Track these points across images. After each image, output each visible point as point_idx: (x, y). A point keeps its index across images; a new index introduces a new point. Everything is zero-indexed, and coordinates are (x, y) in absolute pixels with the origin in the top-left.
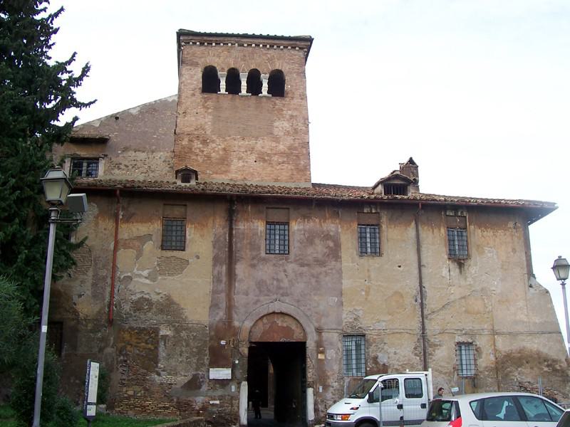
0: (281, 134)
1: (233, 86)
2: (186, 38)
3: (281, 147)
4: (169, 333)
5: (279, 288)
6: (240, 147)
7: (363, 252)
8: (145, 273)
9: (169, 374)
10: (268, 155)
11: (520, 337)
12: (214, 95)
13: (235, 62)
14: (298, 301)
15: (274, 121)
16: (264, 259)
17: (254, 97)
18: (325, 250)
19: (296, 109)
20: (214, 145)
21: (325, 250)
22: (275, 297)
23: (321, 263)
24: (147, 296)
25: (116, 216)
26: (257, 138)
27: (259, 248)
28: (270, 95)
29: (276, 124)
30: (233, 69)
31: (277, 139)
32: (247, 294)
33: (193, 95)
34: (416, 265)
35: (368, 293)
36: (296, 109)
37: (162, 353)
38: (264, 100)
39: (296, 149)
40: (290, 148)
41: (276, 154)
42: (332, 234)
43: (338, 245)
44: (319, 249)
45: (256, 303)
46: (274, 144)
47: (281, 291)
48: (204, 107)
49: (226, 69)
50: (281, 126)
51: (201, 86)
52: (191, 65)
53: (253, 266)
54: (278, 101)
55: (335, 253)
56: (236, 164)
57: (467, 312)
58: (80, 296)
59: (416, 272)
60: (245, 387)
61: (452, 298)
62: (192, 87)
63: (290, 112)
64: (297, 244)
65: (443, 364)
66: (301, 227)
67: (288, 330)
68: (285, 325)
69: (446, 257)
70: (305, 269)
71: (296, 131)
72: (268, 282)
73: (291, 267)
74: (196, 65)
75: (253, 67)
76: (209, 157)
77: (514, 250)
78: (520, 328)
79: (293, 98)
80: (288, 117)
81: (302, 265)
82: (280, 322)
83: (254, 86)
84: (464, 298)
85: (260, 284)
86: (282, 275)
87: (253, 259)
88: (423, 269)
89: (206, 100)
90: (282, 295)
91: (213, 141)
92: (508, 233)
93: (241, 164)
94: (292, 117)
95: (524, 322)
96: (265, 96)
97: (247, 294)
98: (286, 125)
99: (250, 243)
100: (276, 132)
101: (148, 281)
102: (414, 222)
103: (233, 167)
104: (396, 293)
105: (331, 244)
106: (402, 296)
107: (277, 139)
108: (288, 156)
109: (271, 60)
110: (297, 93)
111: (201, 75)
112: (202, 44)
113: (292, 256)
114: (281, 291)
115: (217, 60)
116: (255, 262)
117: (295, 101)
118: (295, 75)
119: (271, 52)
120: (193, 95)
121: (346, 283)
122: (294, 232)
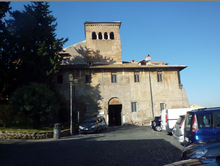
0: (114, 50)
1: (100, 37)
2: (87, 24)
3: (114, 53)
4: (89, 104)
5: (116, 91)
6: (103, 54)
7: (135, 81)
8: (82, 89)
9: (89, 114)
10: (111, 56)
11: (177, 101)
12: (95, 40)
13: (100, 31)
14: (120, 94)
16: (111, 84)
17: (106, 40)
18: (126, 81)
19: (117, 43)
21: (126, 81)
22: (114, 93)
23: (126, 85)
24: (83, 95)
26: (107, 51)
27: (110, 82)
28: (110, 39)
29: (112, 47)
30: (100, 32)
31: (113, 51)
32: (107, 93)
34: (149, 84)
35: (137, 92)
36: (117, 43)
37: (87, 108)
38: (109, 41)
39: (118, 54)
40: (116, 54)
41: (112, 55)
42: (128, 77)
43: (129, 80)
44: (125, 81)
45: (110, 95)
46: (112, 53)
47: (116, 92)
48: (93, 43)
49: (98, 32)
50: (114, 47)
51: (92, 37)
52: (89, 32)
53: (108, 86)
54: (112, 41)
55: (128, 82)
57: (163, 95)
58: (66, 96)
59: (149, 86)
60: (108, 116)
61: (159, 92)
62: (90, 38)
63: (116, 44)
64: (119, 80)
65: (157, 109)
66: (120, 76)
67: (117, 102)
68: (117, 100)
69: (157, 82)
70: (121, 86)
71: (118, 49)
72: (112, 90)
73: (118, 86)
74: (90, 32)
75: (105, 31)
78: (176, 99)
79: (116, 40)
80: (115, 45)
81: (120, 85)
82: (115, 99)
83: (106, 37)
84: (162, 92)
85: (110, 90)
86: (116, 88)
87: (108, 84)
88: (151, 85)
89: (93, 41)
90: (116, 93)
92: (173, 75)
94: (116, 45)
95: (178, 98)
96: (109, 40)
97: (107, 93)
98: (115, 47)
99: (107, 80)
100: (113, 49)
101: (83, 91)
102: (148, 73)
104: (144, 91)
105: (127, 80)
106: (146, 92)
107: (113, 51)
108: (116, 56)
109: (110, 29)
110: (117, 39)
111: (91, 34)
112: (91, 26)
113: (118, 83)
114: (116, 92)
116: (109, 85)
117: (117, 40)
118: (117, 33)
119: (110, 27)
120: (90, 40)
121: (132, 90)
122: (118, 77)
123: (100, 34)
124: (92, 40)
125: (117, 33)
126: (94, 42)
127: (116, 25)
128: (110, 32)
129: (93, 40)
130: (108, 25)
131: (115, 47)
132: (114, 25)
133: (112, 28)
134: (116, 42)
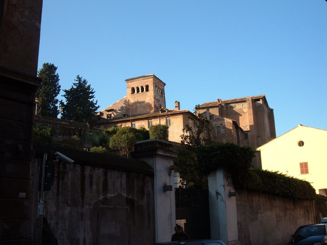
1: (138, 91)
15: (146, 98)
19: (151, 94)
20: (134, 106)
25: (106, 127)
29: (146, 99)
33: (129, 95)
41: (146, 106)
54: (147, 93)
56: (139, 110)
71: (151, 99)
75: (142, 85)
76: (133, 109)
77: (180, 122)
80: (149, 96)
83: (142, 90)
91: (134, 105)
92: (179, 119)
93: (139, 110)
103: (138, 111)
109: (145, 83)
110: (151, 90)
111: (131, 90)
115: (134, 85)
117: (151, 92)
118: (151, 85)
119: (144, 80)
120: (129, 95)
123: (138, 89)
124: (130, 95)
125: (151, 85)
126: (133, 97)
127: (150, 78)
128: (145, 85)
129: (132, 95)
130: (144, 79)
131: (149, 98)
132: (148, 78)
133: (148, 81)
134: (150, 93)
